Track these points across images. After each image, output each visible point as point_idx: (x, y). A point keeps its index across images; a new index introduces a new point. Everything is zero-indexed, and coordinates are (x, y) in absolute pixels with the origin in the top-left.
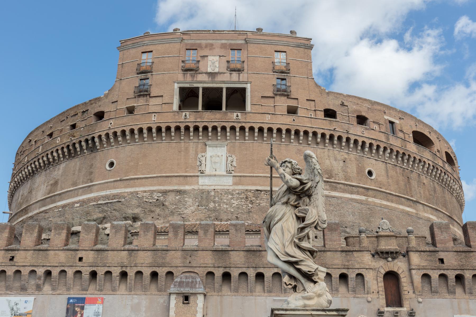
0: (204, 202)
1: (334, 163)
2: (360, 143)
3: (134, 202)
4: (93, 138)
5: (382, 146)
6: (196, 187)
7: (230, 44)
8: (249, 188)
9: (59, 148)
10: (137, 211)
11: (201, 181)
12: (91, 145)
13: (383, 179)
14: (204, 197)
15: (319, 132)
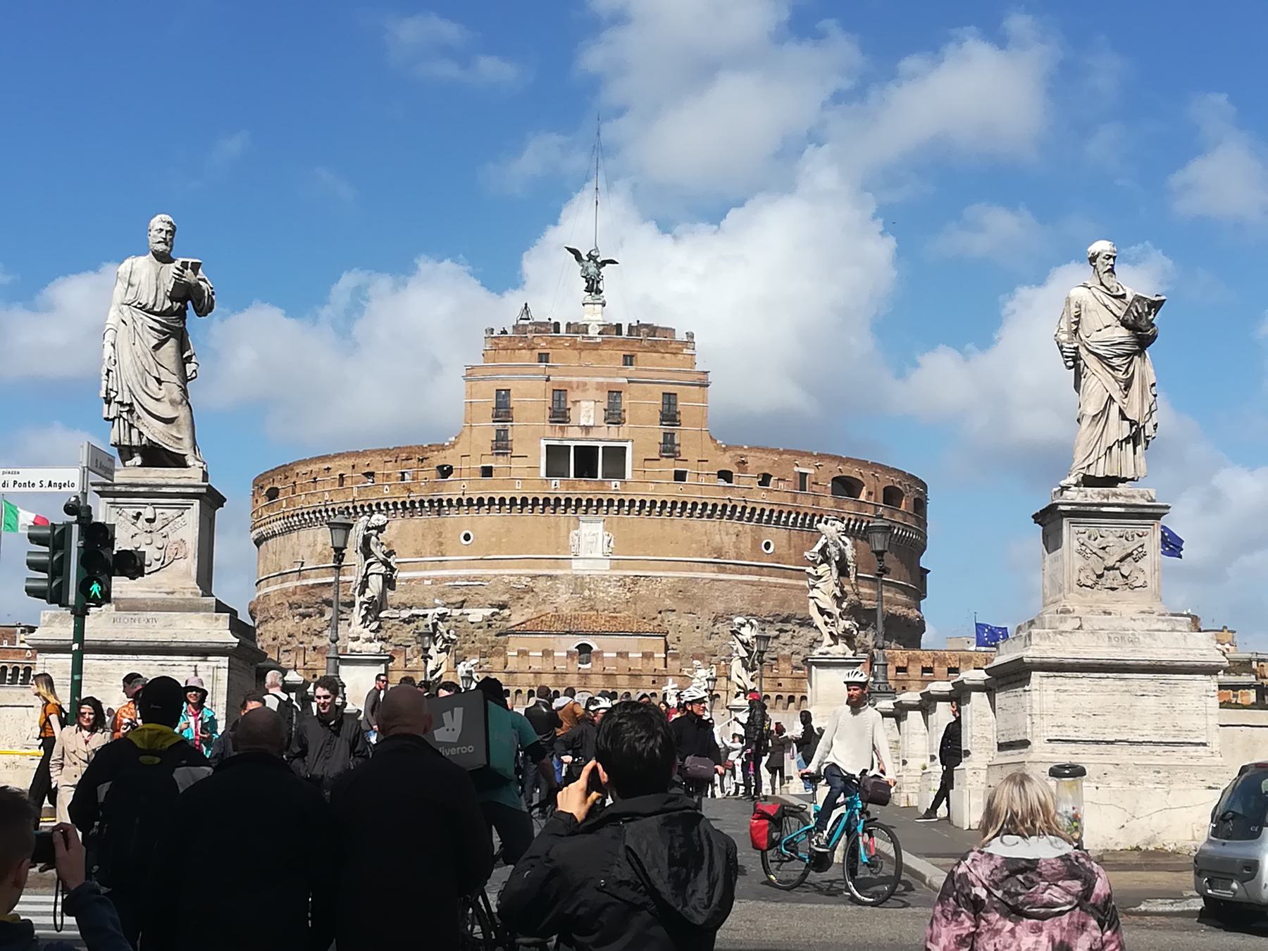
0: (578, 590)
1: (726, 539)
2: (758, 512)
3: (501, 587)
4: (440, 501)
5: (786, 510)
6: (569, 572)
7: (609, 384)
8: (628, 573)
9: (390, 501)
10: (505, 598)
11: (575, 564)
12: (438, 506)
13: (784, 551)
14: (578, 584)
15: (710, 502)
